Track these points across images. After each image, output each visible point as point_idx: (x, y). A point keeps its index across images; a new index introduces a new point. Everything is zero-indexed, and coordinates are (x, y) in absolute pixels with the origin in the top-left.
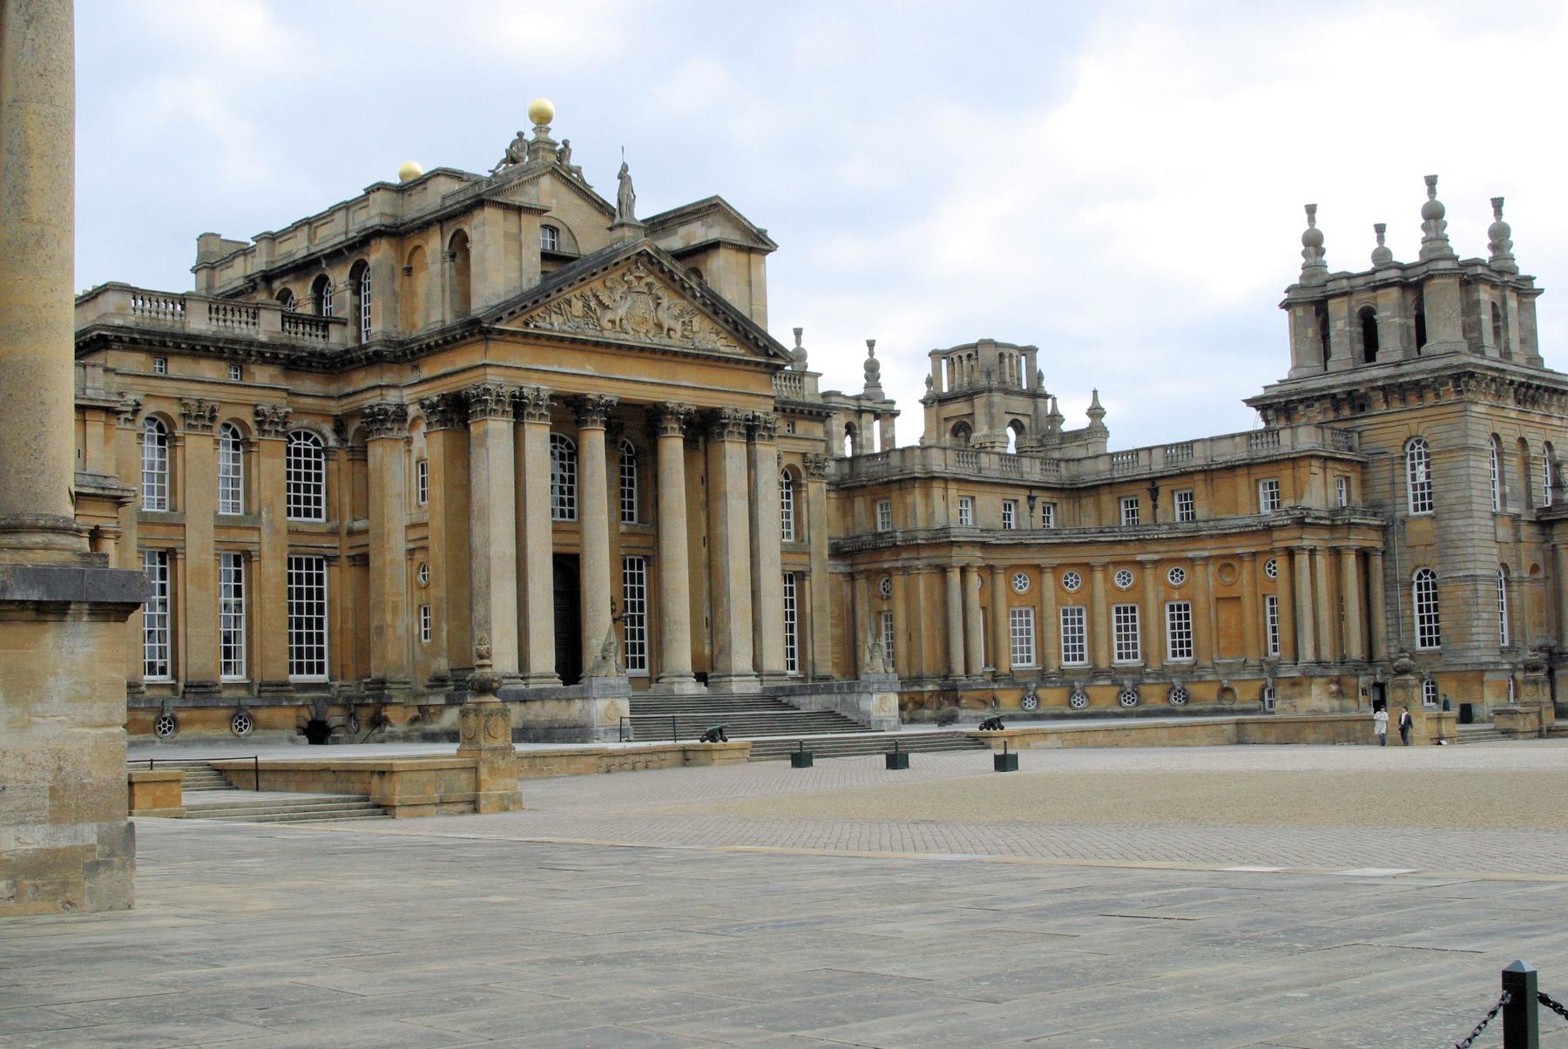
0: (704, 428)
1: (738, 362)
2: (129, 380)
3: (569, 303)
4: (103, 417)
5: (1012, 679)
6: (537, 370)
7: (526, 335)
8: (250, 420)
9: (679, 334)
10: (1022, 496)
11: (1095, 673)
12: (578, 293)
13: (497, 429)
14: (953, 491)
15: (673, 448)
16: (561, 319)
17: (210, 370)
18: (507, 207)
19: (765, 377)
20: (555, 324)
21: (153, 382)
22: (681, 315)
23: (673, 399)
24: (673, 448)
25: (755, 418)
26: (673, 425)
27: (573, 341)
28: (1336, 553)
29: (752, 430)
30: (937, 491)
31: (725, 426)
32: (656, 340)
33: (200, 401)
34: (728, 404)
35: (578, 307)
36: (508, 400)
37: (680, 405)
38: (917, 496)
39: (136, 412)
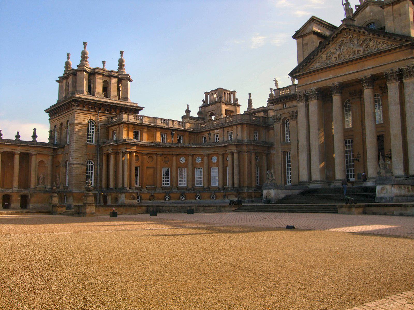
0: (379, 82)
1: (390, 50)
2: (278, 111)
3: (322, 57)
4: (240, 126)
6: (312, 83)
7: (306, 74)
9: (362, 51)
12: (325, 53)
15: (368, 92)
16: (319, 64)
18: (302, 37)
19: (409, 51)
20: (316, 65)
21: (283, 110)
22: (364, 42)
23: (360, 76)
25: (400, 70)
31: (387, 77)
32: (354, 56)
33: (293, 112)
34: (386, 69)
35: (324, 56)
36: (302, 96)
37: (365, 77)
39: (280, 119)
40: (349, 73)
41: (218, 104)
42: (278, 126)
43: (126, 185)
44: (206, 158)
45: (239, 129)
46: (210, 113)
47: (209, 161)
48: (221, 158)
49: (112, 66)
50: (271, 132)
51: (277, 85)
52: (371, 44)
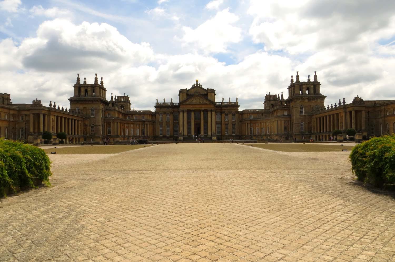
0: (206, 111)
5: (255, 136)
8: (169, 113)
10: (261, 114)
11: (264, 135)
13: (181, 114)
14: (248, 114)
15: (202, 113)
17: (165, 109)
20: (187, 103)
23: (201, 109)
24: (202, 113)
26: (202, 111)
27: (189, 105)
28: (282, 120)
29: (211, 111)
30: (246, 115)
38: (244, 115)
40: (198, 107)
41: (126, 103)
42: (157, 116)
43: (119, 134)
44: (135, 125)
45: (148, 116)
46: (120, 106)
47: (136, 126)
48: (141, 126)
49: (91, 81)
50: (154, 117)
51: (157, 101)
52: (204, 101)
